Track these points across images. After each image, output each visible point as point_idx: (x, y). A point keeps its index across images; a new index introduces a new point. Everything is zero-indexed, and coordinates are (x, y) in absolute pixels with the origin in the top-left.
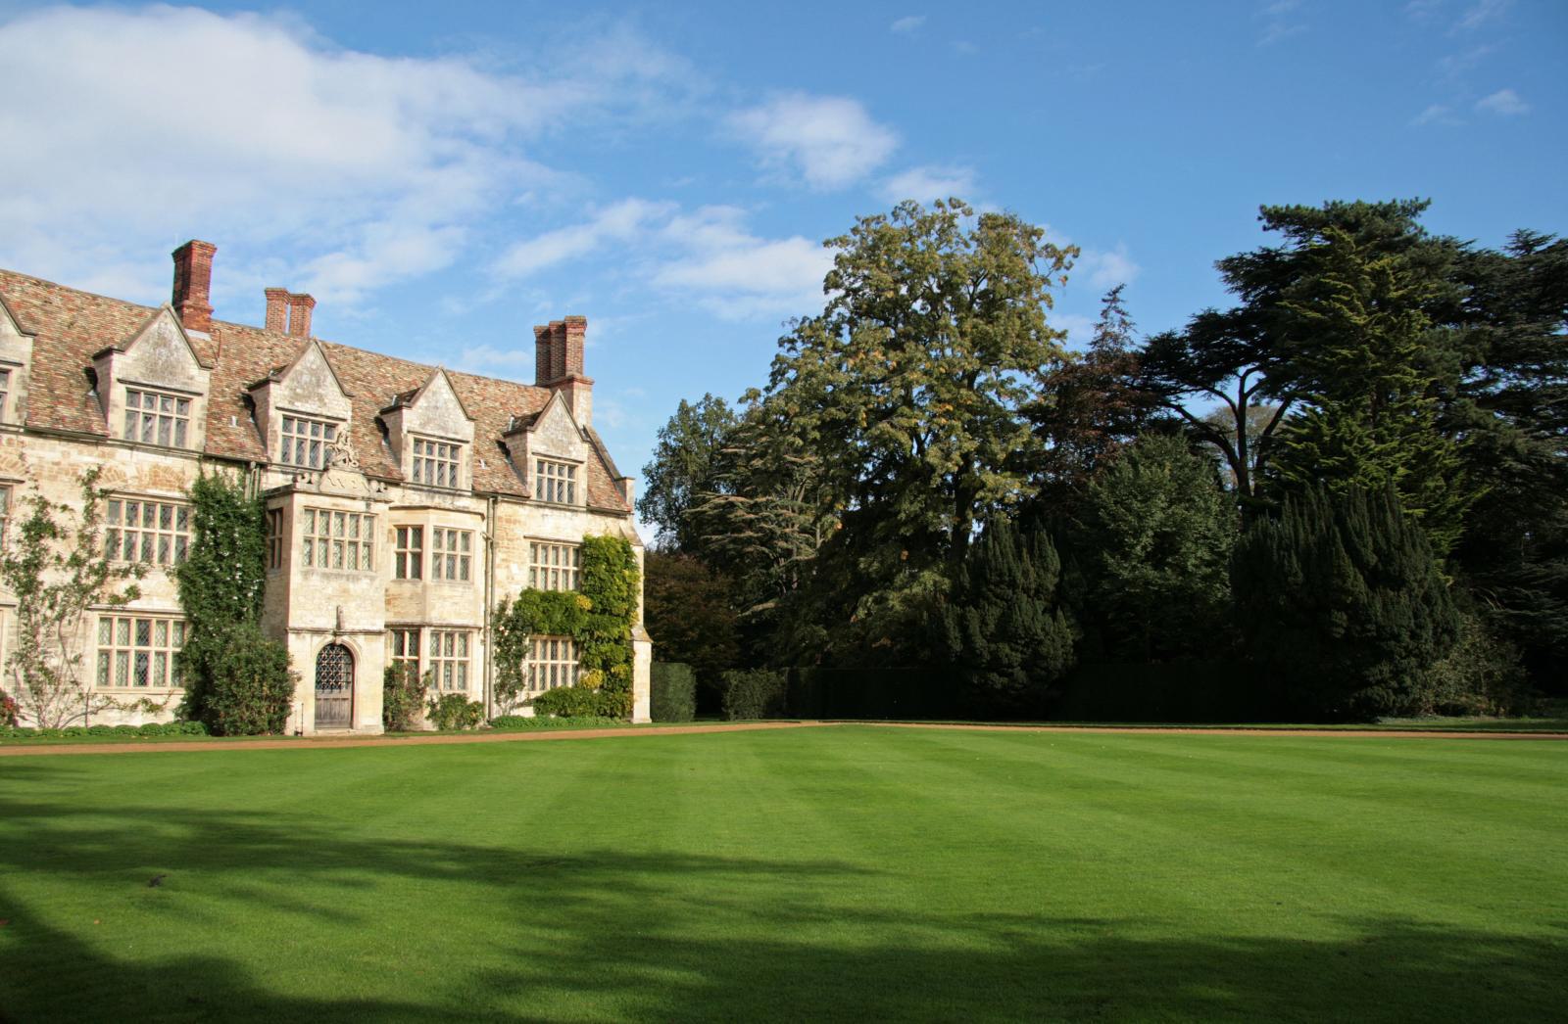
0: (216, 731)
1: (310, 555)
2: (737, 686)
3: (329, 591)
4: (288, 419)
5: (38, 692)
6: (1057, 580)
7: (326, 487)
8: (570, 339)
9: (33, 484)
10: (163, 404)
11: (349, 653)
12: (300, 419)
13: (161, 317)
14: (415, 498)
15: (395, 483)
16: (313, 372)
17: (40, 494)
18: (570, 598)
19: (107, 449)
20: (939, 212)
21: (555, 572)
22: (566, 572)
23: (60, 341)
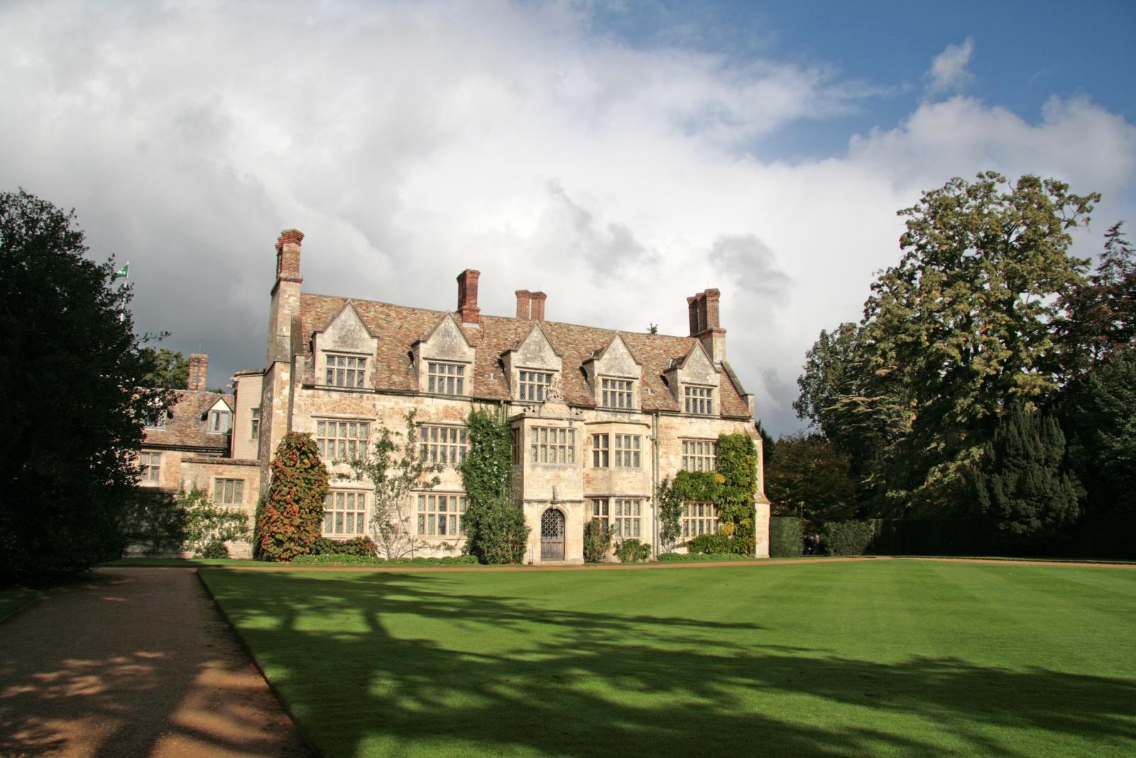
0: (483, 562)
1: (536, 455)
2: (835, 533)
3: (548, 477)
4: (523, 374)
5: (386, 538)
6: (1063, 452)
7: (544, 413)
8: (709, 304)
9: (380, 421)
10: (449, 369)
11: (562, 514)
12: (530, 373)
13: (446, 319)
14: (604, 416)
15: (592, 408)
16: (537, 343)
17: (384, 426)
18: (710, 475)
19: (419, 399)
20: (980, 181)
21: (700, 459)
22: (708, 459)
23: (395, 338)
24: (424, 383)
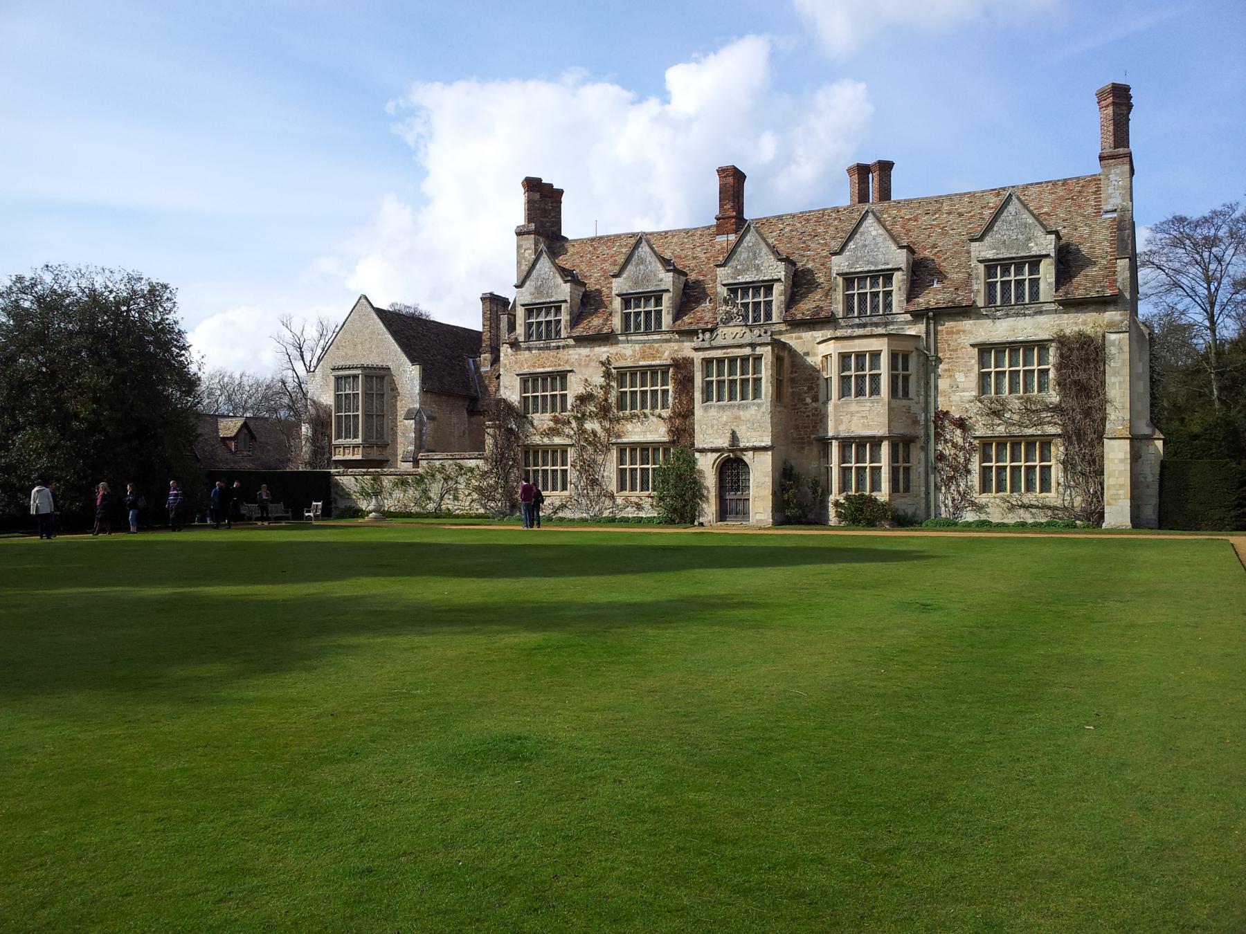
7: (719, 341)
16: (749, 249)
24: (617, 322)
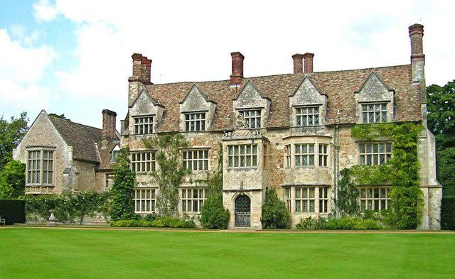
3: (238, 175)
11: (249, 199)
15: (287, 128)
24: (182, 126)
